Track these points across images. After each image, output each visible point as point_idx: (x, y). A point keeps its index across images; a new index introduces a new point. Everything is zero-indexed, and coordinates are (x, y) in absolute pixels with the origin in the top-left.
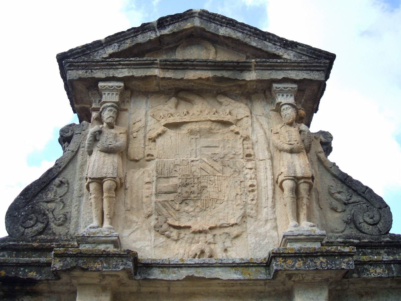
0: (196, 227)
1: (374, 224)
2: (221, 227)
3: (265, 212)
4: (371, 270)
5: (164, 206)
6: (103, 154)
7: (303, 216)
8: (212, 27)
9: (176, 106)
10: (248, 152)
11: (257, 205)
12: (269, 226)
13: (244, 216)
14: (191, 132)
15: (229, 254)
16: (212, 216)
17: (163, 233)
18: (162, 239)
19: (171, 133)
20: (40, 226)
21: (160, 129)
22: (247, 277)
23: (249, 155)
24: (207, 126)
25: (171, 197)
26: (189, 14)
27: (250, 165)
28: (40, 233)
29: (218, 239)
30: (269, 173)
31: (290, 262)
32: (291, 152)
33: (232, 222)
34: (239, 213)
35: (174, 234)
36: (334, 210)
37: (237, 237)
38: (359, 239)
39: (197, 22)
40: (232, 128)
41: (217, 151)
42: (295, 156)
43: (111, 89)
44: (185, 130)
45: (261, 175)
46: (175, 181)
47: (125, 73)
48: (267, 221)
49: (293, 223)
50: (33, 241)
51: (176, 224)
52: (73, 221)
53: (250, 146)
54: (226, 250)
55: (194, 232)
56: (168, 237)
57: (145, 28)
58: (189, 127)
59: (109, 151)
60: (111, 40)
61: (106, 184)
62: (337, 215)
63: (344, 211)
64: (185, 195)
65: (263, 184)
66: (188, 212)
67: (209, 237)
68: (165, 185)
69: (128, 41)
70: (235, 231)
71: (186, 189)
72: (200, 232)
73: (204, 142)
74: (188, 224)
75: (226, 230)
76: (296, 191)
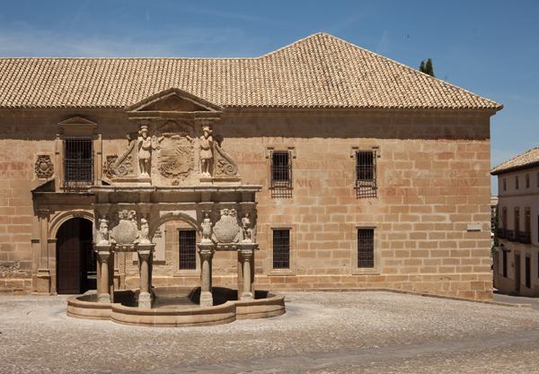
68: (164, 158)
76: (206, 163)
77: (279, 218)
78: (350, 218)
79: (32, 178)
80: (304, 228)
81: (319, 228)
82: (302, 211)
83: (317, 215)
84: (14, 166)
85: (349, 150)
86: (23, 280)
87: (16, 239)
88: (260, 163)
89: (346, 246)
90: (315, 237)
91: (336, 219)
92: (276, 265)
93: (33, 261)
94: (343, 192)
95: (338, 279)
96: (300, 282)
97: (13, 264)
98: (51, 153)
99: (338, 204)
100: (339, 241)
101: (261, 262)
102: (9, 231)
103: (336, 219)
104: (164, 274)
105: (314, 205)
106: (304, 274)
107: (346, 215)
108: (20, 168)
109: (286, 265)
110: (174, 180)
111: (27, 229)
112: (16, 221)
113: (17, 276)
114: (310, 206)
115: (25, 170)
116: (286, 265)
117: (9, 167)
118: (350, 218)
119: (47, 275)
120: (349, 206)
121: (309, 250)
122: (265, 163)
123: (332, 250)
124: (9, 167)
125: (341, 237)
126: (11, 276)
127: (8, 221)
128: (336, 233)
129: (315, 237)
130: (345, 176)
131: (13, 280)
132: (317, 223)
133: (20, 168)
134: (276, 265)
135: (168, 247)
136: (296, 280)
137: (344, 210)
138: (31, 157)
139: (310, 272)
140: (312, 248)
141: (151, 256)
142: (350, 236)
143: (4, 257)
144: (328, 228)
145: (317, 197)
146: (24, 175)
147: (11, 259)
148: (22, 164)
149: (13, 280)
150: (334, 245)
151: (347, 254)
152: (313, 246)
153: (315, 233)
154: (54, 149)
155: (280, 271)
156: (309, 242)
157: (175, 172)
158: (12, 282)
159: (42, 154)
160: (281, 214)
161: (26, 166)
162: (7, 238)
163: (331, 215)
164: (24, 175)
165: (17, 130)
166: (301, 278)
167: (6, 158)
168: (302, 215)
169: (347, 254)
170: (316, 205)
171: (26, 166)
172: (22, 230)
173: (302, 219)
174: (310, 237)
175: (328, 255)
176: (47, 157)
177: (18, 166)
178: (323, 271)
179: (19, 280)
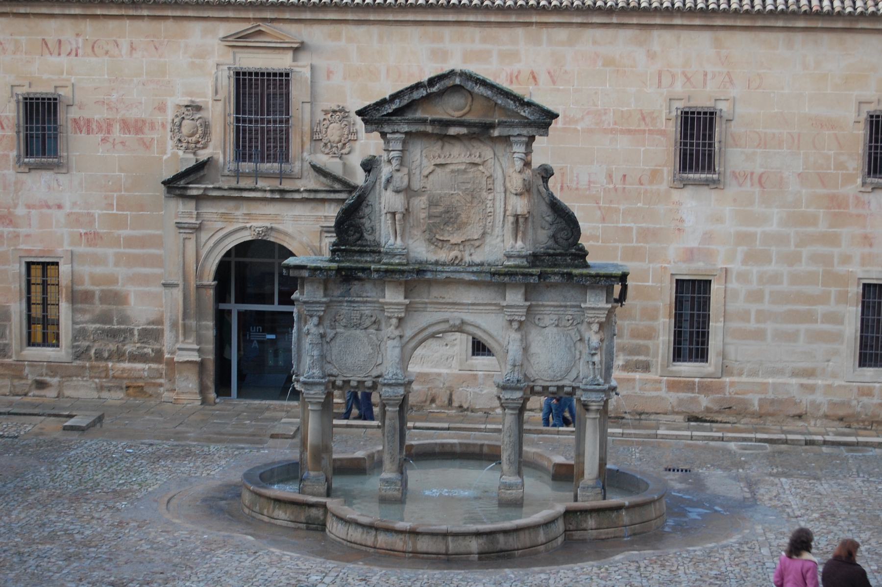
0: (453, 241)
1: (567, 240)
2: (469, 240)
3: (498, 230)
4: (552, 277)
5: (434, 226)
6: (394, 194)
7: (519, 238)
8: (469, 85)
9: (442, 148)
10: (489, 187)
11: (492, 226)
12: (499, 239)
13: (484, 234)
14: (452, 171)
15: (473, 257)
16: (464, 234)
17: (433, 244)
18: (433, 247)
19: (438, 170)
20: (357, 235)
21: (432, 168)
22: (480, 279)
23: (490, 189)
24: (463, 167)
25: (438, 220)
26: (452, 73)
27: (490, 197)
28: (358, 240)
29: (467, 248)
30: (502, 203)
31: (502, 277)
32: (516, 194)
33: (476, 237)
34: (481, 232)
35: (440, 244)
36: (543, 228)
37: (478, 247)
38: (555, 250)
39: (458, 81)
40: (481, 168)
41: (469, 186)
42: (518, 198)
43: (396, 139)
44: (448, 169)
45: (497, 204)
46: (440, 209)
47: (406, 128)
48: (498, 236)
49: (512, 242)
50: (355, 246)
51: (441, 238)
52: (377, 233)
53: (491, 182)
54: (471, 255)
55: (452, 244)
56: (436, 246)
57: (418, 86)
58: (452, 167)
59: (397, 191)
60: (394, 97)
61: (398, 217)
62: (545, 232)
63: (549, 229)
64: (447, 219)
65: (498, 211)
66: (448, 231)
67: (461, 247)
69: (406, 97)
70: (477, 243)
71: (448, 215)
72: (455, 244)
73: (461, 178)
74: (448, 239)
75: (472, 242)
77: (690, 255)
78: (846, 259)
79: (164, 152)
80: (743, 277)
81: (775, 279)
82: (743, 238)
83: (774, 248)
84: (126, 126)
85: (853, 108)
87: (133, 279)
88: (651, 132)
89: (832, 318)
90: (767, 297)
91: (814, 258)
92: (678, 355)
93: (167, 327)
94: (835, 202)
95: (812, 389)
96: (729, 392)
97: (124, 331)
98: (206, 98)
99: (822, 227)
100: (820, 309)
101: (647, 347)
102: (117, 264)
103: (814, 258)
105: (767, 229)
106: (740, 374)
107: (836, 251)
109: (701, 355)
110: (453, 254)
111: (156, 261)
112: (130, 242)
114: (759, 230)
115: (148, 135)
116: (701, 355)
117: (117, 127)
118: (846, 259)
120: (845, 232)
121: (753, 325)
122: (662, 133)
123: (803, 327)
124: (117, 127)
125: (823, 299)
127: (116, 242)
128: (815, 290)
129: (767, 297)
130: (840, 166)
132: (772, 268)
134: (678, 355)
136: (721, 388)
137: (832, 240)
138: (162, 108)
139: (753, 373)
140: (758, 321)
141: (405, 399)
142: (843, 298)
143: (105, 318)
144: (795, 279)
145: (776, 210)
146: (147, 146)
148: (144, 121)
150: (808, 317)
151: (836, 337)
152: (762, 316)
153: (768, 289)
154: (210, 91)
155: (686, 368)
156: (754, 308)
157: (455, 239)
159: (186, 101)
160: (693, 244)
161: (152, 127)
162: (113, 280)
163: (806, 252)
164: (147, 146)
165: (132, 48)
166: (732, 384)
167: (110, 108)
168: (741, 249)
169: (836, 337)
170: (773, 227)
172: (143, 261)
173: (739, 257)
174: (755, 296)
175: (792, 337)
176: (198, 108)
177: (135, 127)
178: (780, 372)
179: (139, 366)
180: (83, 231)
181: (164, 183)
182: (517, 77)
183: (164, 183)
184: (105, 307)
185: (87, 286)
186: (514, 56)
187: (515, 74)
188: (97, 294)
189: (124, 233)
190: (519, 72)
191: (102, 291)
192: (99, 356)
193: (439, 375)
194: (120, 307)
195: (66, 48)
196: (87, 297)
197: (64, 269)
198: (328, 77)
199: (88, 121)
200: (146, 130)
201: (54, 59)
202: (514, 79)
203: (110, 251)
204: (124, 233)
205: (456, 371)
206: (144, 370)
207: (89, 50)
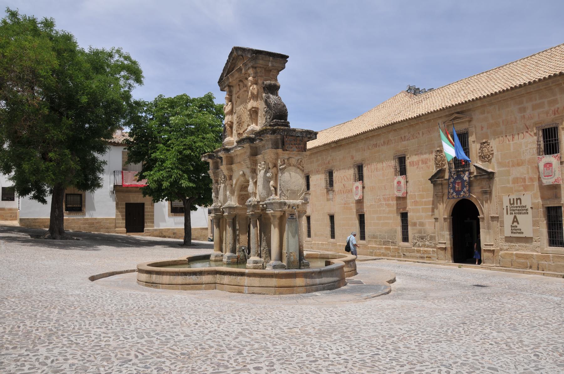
86: (431, 249)
97: (425, 236)
104: (532, 251)
108: (426, 163)
113: (428, 247)
117: (420, 163)
119: (444, 246)
124: (420, 163)
126: (424, 246)
131: (426, 249)
133: (426, 163)
135: (535, 223)
147: (424, 233)
148: (427, 159)
149: (426, 249)
158: (425, 251)
161: (430, 161)
165: (423, 134)
171: (430, 161)
179: (429, 249)
180: (413, 201)
181: (429, 179)
182: (557, 111)
183: (429, 179)
184: (420, 227)
185: (415, 220)
186: (555, 101)
187: (556, 109)
188: (418, 223)
189: (424, 200)
190: (558, 108)
191: (419, 222)
192: (419, 246)
193: (532, 255)
194: (424, 228)
195: (407, 138)
196: (415, 224)
197: (409, 214)
198: (482, 130)
199: (413, 162)
200: (428, 162)
201: (404, 143)
202: (556, 112)
203: (420, 207)
204: (424, 200)
205: (540, 254)
206: (430, 251)
207: (412, 138)
